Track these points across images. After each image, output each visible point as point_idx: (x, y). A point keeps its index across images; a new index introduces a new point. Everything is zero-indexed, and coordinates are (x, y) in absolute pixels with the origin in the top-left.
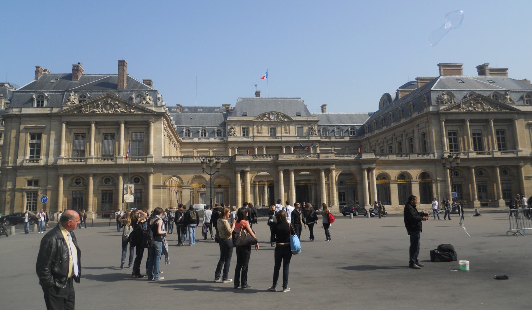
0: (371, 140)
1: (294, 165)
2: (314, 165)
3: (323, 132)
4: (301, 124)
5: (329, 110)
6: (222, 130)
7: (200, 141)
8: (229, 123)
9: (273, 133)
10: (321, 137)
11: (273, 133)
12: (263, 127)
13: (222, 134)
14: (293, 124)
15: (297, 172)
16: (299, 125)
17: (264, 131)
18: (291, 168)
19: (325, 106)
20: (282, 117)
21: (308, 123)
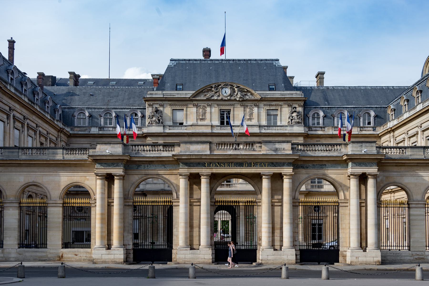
0: (397, 133)
1: (209, 165)
2: (249, 165)
3: (313, 118)
4: (276, 105)
5: (328, 82)
6: (139, 114)
7: (101, 132)
8: (151, 103)
9: (225, 119)
10: (310, 128)
11: (225, 119)
12: (208, 109)
13: (139, 120)
14: (261, 104)
15: (214, 179)
16: (270, 105)
17: (208, 116)
18: (205, 171)
19: (323, 73)
20: (241, 90)
21: (289, 102)
